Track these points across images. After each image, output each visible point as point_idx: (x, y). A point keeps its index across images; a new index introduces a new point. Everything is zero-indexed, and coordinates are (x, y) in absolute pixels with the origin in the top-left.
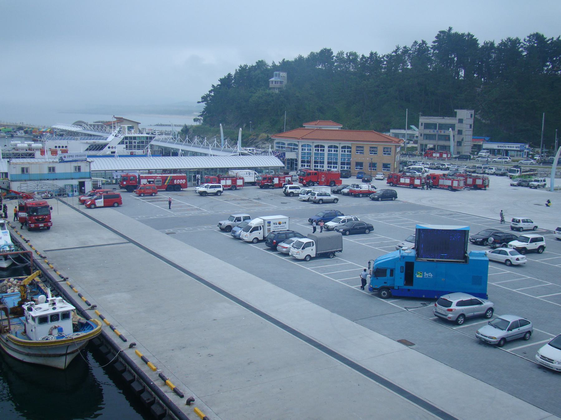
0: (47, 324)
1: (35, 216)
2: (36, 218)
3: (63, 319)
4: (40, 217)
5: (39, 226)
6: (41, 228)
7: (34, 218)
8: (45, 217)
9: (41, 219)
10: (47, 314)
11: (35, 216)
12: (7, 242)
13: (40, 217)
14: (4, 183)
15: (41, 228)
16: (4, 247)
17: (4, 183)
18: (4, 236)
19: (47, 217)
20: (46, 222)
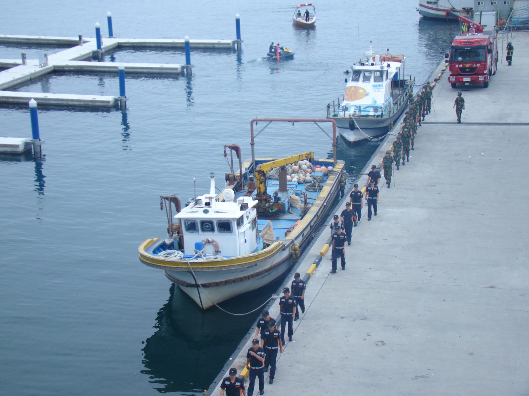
0: (212, 233)
1: (459, 63)
2: (461, 66)
3: (230, 230)
4: (468, 66)
5: (463, 81)
6: (465, 84)
7: (457, 66)
8: (475, 66)
9: (468, 68)
10: (230, 219)
11: (459, 63)
12: (375, 101)
13: (468, 66)
14: (505, 3)
15: (465, 84)
16: (367, 109)
17: (505, 3)
18: (375, 91)
19: (478, 65)
20: (475, 74)
